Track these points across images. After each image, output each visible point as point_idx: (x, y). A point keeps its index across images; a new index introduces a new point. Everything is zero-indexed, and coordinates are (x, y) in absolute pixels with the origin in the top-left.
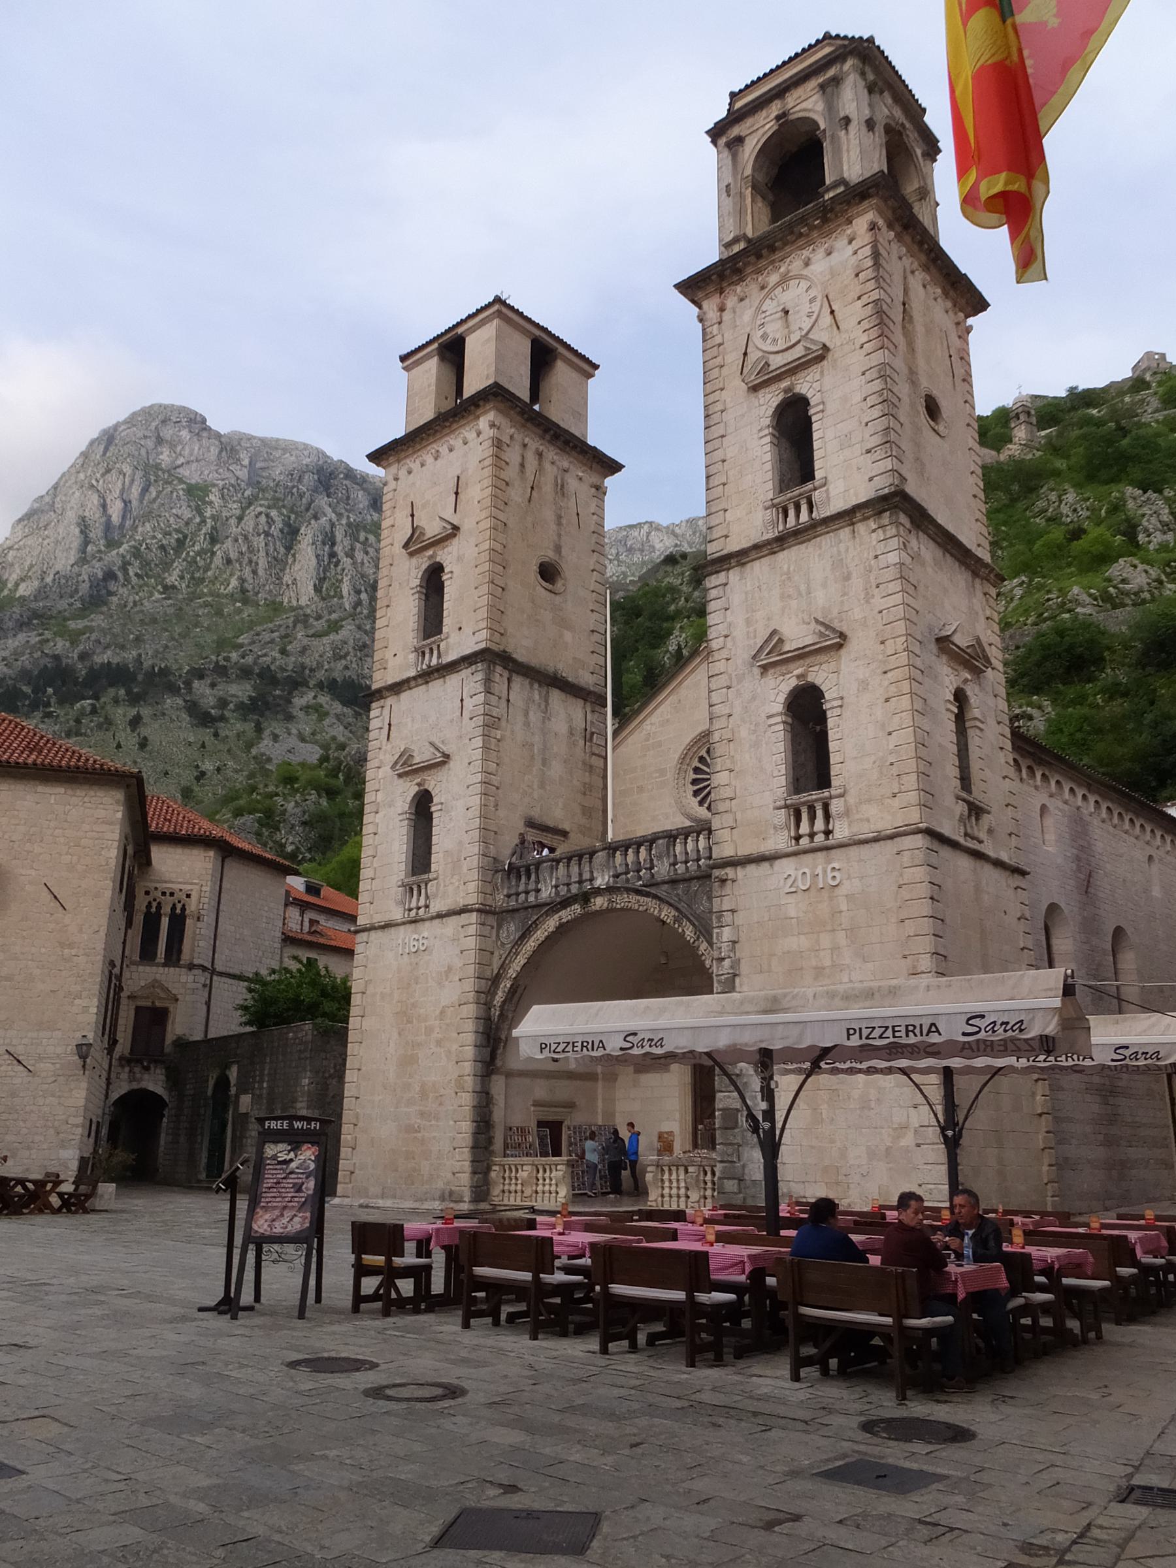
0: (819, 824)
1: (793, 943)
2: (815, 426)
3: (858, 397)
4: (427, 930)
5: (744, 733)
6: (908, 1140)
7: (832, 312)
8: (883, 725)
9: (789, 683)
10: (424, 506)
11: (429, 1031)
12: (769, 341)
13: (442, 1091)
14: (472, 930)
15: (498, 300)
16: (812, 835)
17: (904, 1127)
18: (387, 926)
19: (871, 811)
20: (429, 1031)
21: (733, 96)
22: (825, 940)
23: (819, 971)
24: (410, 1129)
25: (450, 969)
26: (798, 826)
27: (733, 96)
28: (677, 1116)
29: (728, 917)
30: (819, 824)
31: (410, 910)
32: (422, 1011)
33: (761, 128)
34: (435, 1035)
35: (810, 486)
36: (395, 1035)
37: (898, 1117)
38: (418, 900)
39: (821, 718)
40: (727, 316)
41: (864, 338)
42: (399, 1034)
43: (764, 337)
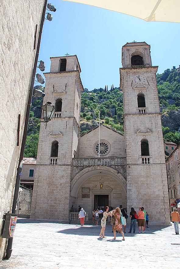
0: (147, 161)
1: (142, 179)
2: (145, 99)
3: (153, 97)
4: (57, 167)
5: (133, 144)
6: (163, 210)
7: (148, 83)
8: (159, 148)
9: (142, 138)
10: (56, 86)
11: (58, 187)
12: (136, 83)
13: (61, 199)
14: (70, 169)
15: (76, 56)
16: (146, 163)
17: (162, 209)
18: (46, 165)
19: (157, 160)
20: (58, 187)
21: (127, 43)
22: (149, 180)
23: (147, 184)
24: (51, 206)
25: (63, 176)
26: (143, 161)
27: (127, 43)
28: (91, 206)
29: (130, 174)
30: (147, 161)
31: (51, 163)
32: (55, 183)
33: (133, 50)
34: (59, 188)
35: (145, 108)
36: (47, 187)
37: (161, 207)
38: (54, 162)
39: (148, 145)
40: (128, 76)
41: (154, 89)
42: (49, 187)
43: (135, 82)
